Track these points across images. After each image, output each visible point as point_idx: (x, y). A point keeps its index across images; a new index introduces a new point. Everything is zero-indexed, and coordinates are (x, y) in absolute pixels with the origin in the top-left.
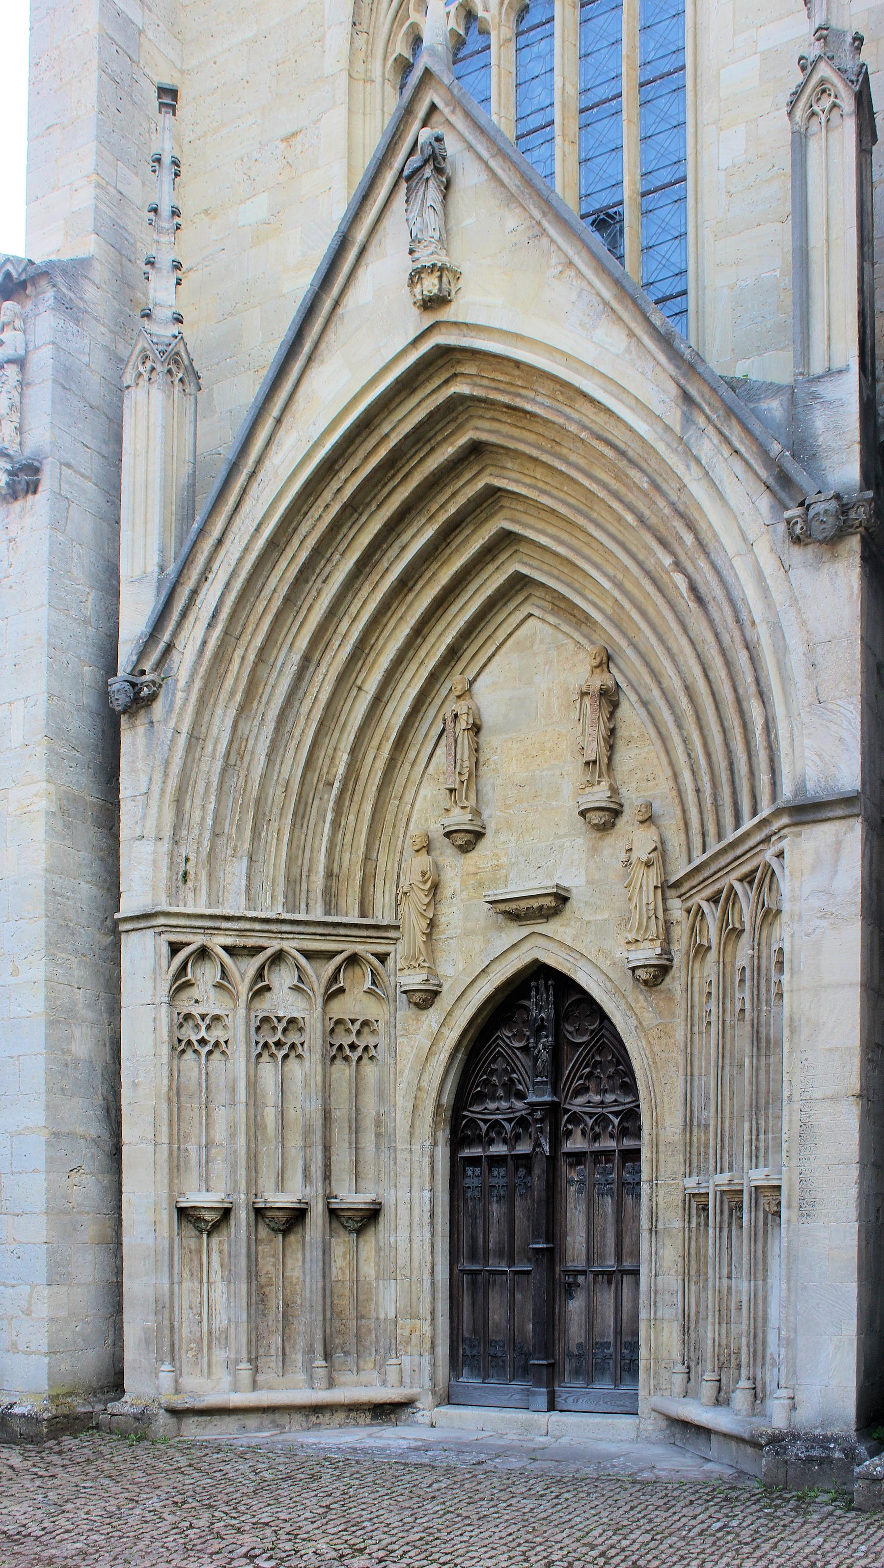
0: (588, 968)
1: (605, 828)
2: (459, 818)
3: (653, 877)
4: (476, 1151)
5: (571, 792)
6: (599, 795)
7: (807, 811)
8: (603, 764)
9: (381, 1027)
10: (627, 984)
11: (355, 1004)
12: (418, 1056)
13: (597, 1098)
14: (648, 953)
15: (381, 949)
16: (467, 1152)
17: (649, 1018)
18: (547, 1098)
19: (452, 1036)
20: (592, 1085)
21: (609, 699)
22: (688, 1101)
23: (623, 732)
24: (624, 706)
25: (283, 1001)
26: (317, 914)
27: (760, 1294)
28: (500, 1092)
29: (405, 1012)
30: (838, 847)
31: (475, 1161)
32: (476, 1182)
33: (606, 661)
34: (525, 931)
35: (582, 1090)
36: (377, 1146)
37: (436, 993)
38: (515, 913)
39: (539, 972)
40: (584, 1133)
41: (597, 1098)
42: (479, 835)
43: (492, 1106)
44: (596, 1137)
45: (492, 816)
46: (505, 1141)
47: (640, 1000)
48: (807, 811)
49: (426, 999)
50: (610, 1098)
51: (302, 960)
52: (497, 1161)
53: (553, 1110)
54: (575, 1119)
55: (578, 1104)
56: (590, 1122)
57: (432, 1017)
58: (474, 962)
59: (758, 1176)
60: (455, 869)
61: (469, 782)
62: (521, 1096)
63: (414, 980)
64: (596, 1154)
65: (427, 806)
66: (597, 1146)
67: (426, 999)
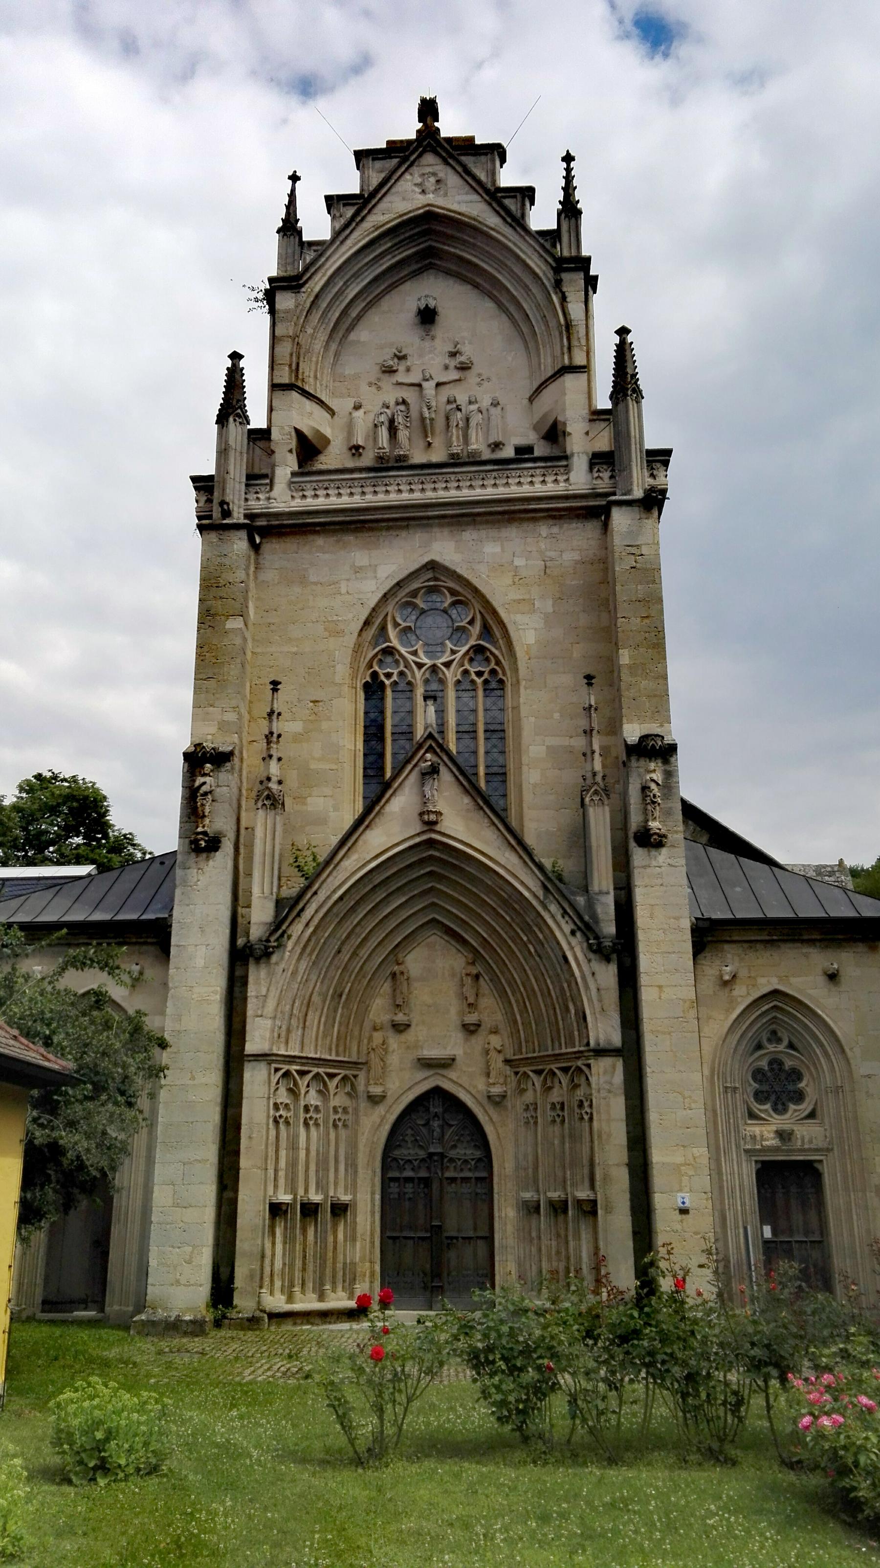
0: (463, 1091)
1: (472, 1032)
2: (400, 1018)
3: (501, 1058)
4: (396, 1174)
6: (472, 1018)
7: (600, 1052)
9: (350, 1110)
10: (485, 1101)
12: (374, 1127)
13: (463, 1152)
14: (496, 1090)
15: (355, 1073)
16: (391, 1174)
17: (495, 1117)
18: (439, 1150)
19: (392, 1118)
20: (459, 1145)
22: (516, 1158)
23: (481, 991)
24: (481, 979)
26: (333, 1057)
27: (298, 1263)
28: (410, 1145)
29: (363, 1104)
30: (614, 1067)
31: (392, 1179)
32: (397, 1190)
34: (431, 1072)
35: (454, 1147)
36: (346, 1170)
37: (384, 1097)
38: (427, 1064)
39: (437, 1092)
40: (455, 1167)
41: (463, 1152)
42: (409, 1026)
43: (405, 1152)
44: (462, 1170)
45: (415, 1018)
46: (413, 1169)
47: (491, 1110)
48: (600, 1052)
50: (468, 1152)
51: (326, 1078)
52: (408, 1180)
53: (442, 1156)
54: (451, 1160)
55: (452, 1154)
56: (459, 1163)
57: (381, 1109)
58: (402, 1085)
60: (394, 1042)
62: (421, 1147)
63: (376, 1090)
64: (463, 1179)
65: (379, 1009)
66: (462, 1175)
67: (375, 1100)
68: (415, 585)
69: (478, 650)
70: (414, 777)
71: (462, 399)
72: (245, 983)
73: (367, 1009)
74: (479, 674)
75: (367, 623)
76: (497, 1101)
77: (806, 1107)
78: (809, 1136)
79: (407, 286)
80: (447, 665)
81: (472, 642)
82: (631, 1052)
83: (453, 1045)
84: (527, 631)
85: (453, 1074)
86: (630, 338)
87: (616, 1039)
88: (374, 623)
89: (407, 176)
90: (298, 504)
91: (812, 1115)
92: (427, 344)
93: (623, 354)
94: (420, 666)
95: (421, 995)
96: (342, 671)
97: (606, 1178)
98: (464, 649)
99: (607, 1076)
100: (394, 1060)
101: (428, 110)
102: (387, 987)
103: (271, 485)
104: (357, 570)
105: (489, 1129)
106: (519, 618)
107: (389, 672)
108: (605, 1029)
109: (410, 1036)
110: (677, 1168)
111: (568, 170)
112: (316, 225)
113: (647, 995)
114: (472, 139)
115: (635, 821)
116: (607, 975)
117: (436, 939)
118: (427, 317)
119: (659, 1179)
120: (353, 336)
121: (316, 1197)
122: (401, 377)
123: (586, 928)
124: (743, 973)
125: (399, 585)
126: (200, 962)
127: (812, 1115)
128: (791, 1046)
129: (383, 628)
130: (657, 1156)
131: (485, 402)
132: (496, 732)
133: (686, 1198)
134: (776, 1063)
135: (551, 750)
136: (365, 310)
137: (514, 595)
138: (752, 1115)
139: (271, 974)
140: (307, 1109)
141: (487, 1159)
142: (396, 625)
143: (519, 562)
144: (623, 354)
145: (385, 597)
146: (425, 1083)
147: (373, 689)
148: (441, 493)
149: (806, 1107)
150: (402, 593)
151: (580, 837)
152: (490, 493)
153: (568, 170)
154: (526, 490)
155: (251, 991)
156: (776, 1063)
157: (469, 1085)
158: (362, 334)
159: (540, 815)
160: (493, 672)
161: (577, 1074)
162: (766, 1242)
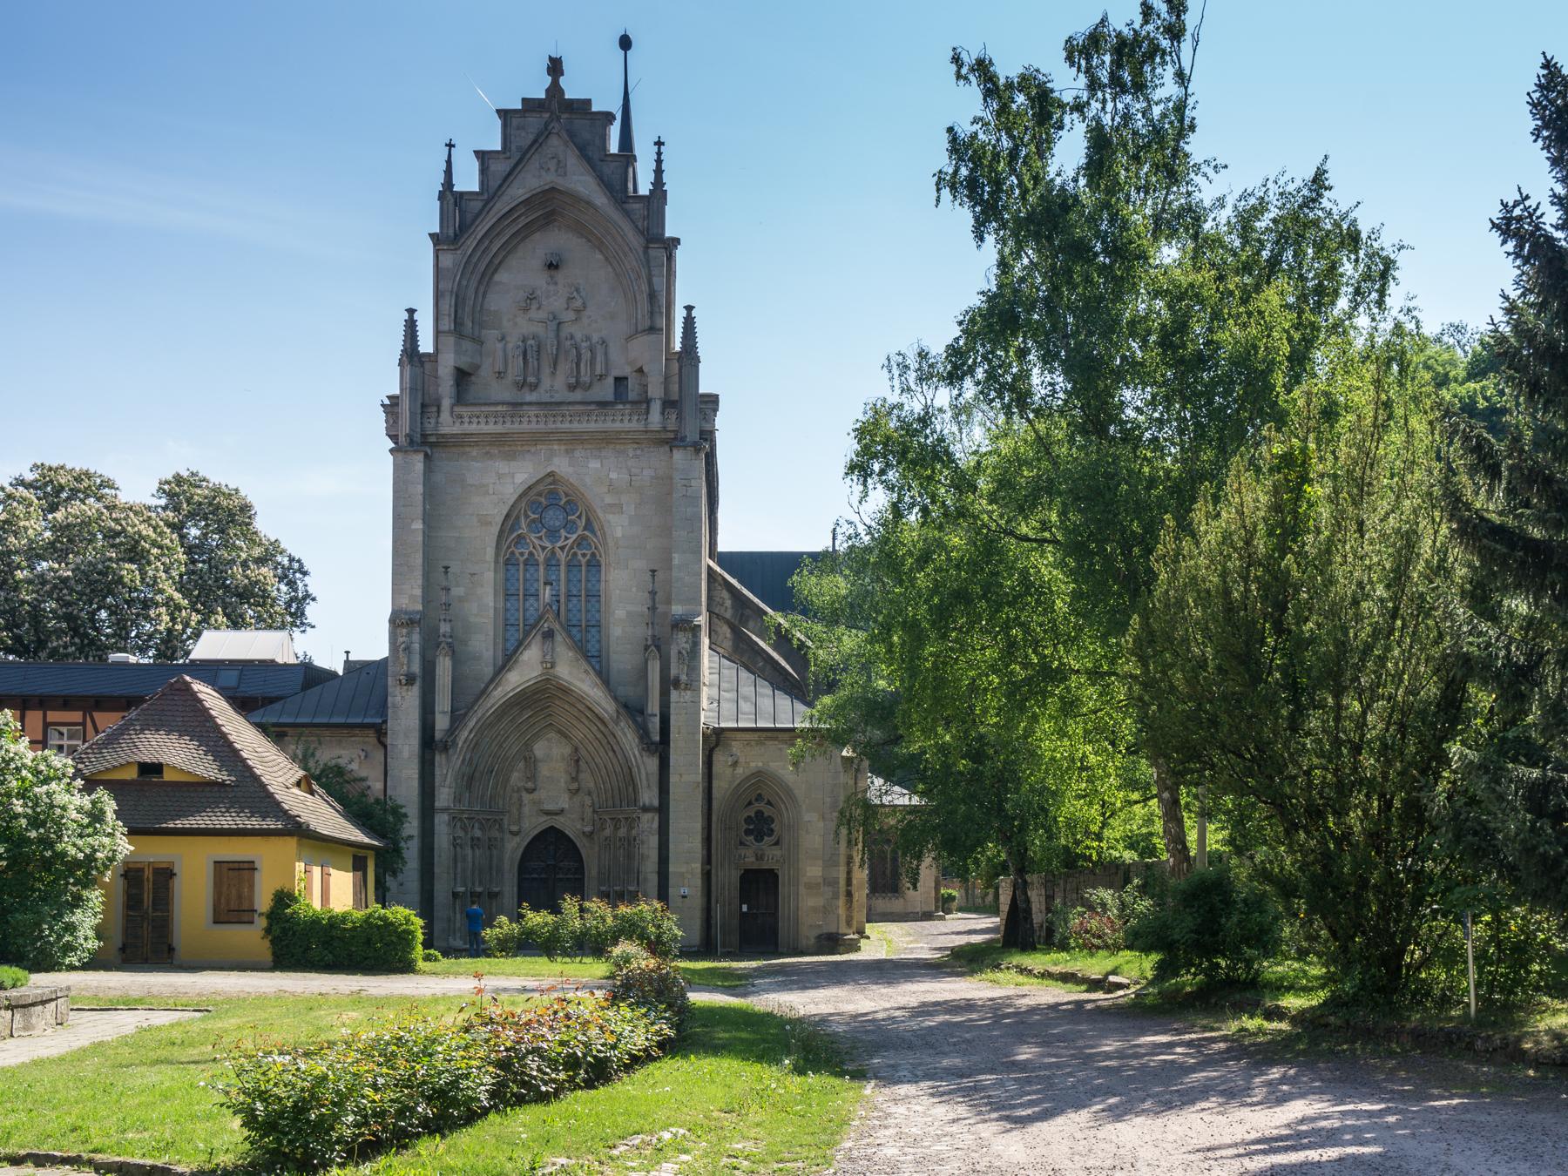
2: (530, 785)
5: (563, 779)
6: (575, 786)
7: (645, 809)
8: (575, 779)
11: (495, 834)
12: (513, 848)
14: (588, 829)
21: (577, 761)
25: (478, 833)
29: (508, 836)
33: (576, 750)
38: (548, 813)
39: (552, 828)
48: (645, 809)
49: (514, 834)
57: (517, 839)
58: (533, 824)
59: (631, 888)
60: (526, 797)
61: (532, 776)
63: (514, 828)
65: (516, 778)
67: (514, 834)
68: (541, 487)
69: (583, 538)
70: (539, 637)
71: (578, 336)
72: (433, 764)
73: (508, 780)
74: (584, 555)
75: (507, 516)
76: (590, 835)
77: (774, 838)
78: (772, 856)
79: (537, 236)
80: (562, 548)
81: (580, 532)
82: (663, 810)
83: (564, 802)
84: (618, 526)
85: (561, 819)
86: (694, 313)
87: (656, 803)
88: (510, 522)
89: (536, 156)
90: (456, 429)
91: (777, 843)
92: (552, 288)
93: (689, 323)
94: (544, 548)
95: (544, 771)
96: (490, 553)
97: (645, 879)
98: (574, 536)
99: (649, 822)
100: (526, 810)
101: (555, 67)
102: (521, 765)
103: (439, 412)
104: (500, 476)
105: (583, 852)
106: (610, 517)
107: (522, 552)
108: (649, 796)
109: (535, 796)
110: (682, 874)
111: (659, 154)
112: (468, 180)
113: (673, 779)
114: (589, 101)
115: (673, 672)
116: (652, 764)
117: (552, 735)
118: (552, 266)
119: (671, 882)
120: (497, 278)
121: (479, 889)
122: (533, 314)
123: (643, 733)
124: (742, 760)
125: (530, 488)
126: (406, 754)
127: (777, 843)
128: (769, 803)
129: (518, 518)
130: (673, 868)
131: (595, 338)
132: (594, 596)
133: (684, 890)
134: (759, 813)
135: (629, 613)
136: (505, 257)
137: (608, 500)
138: (741, 843)
139: (448, 760)
140: (472, 839)
141: (580, 869)
142: (527, 516)
143: (613, 475)
144: (689, 323)
145: (520, 497)
146: (543, 823)
147: (510, 562)
148: (559, 425)
149: (774, 838)
150: (532, 493)
151: (643, 674)
152: (592, 426)
153: (659, 154)
154: (617, 426)
155: (437, 772)
156: (759, 813)
157: (571, 826)
158: (502, 277)
159: (622, 657)
160: (593, 554)
161: (632, 822)
162: (743, 914)
